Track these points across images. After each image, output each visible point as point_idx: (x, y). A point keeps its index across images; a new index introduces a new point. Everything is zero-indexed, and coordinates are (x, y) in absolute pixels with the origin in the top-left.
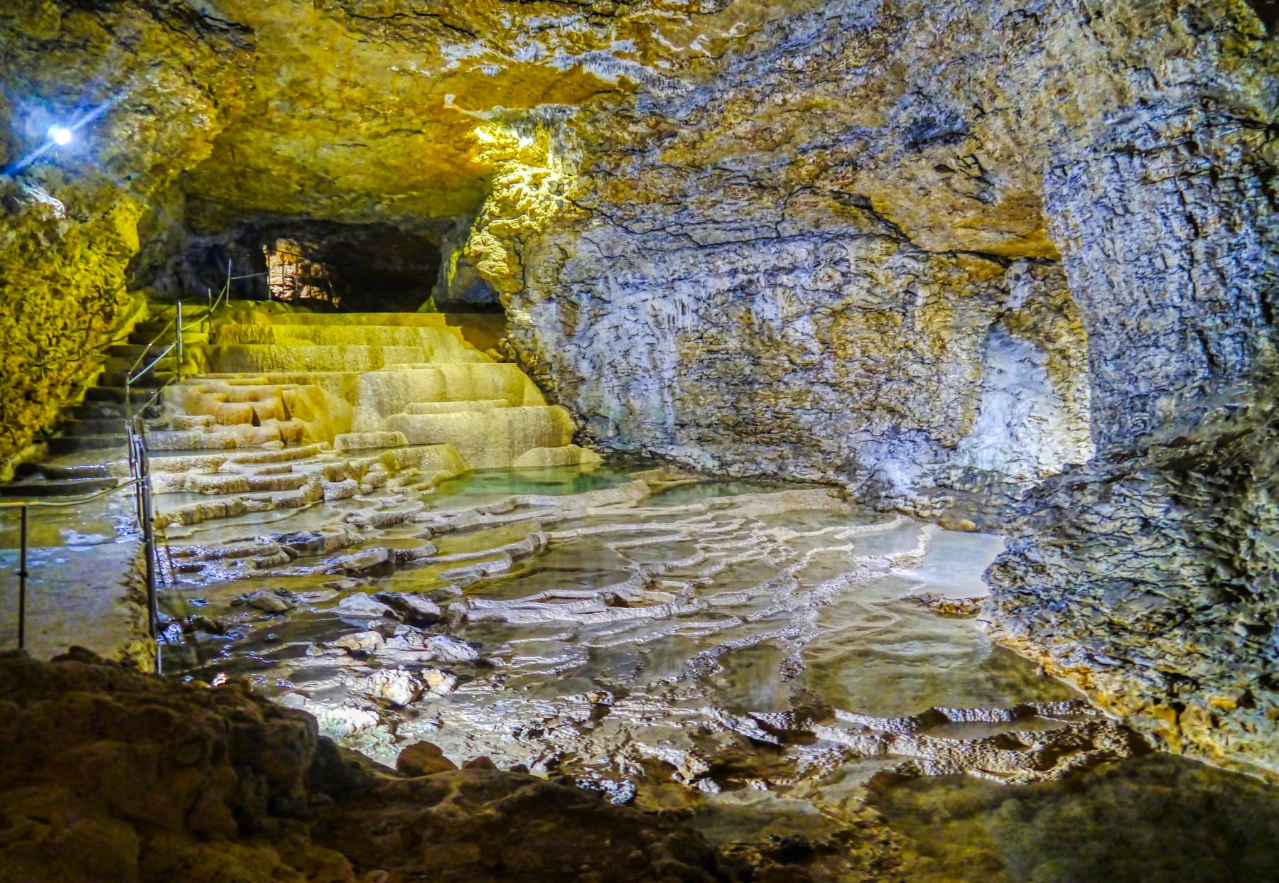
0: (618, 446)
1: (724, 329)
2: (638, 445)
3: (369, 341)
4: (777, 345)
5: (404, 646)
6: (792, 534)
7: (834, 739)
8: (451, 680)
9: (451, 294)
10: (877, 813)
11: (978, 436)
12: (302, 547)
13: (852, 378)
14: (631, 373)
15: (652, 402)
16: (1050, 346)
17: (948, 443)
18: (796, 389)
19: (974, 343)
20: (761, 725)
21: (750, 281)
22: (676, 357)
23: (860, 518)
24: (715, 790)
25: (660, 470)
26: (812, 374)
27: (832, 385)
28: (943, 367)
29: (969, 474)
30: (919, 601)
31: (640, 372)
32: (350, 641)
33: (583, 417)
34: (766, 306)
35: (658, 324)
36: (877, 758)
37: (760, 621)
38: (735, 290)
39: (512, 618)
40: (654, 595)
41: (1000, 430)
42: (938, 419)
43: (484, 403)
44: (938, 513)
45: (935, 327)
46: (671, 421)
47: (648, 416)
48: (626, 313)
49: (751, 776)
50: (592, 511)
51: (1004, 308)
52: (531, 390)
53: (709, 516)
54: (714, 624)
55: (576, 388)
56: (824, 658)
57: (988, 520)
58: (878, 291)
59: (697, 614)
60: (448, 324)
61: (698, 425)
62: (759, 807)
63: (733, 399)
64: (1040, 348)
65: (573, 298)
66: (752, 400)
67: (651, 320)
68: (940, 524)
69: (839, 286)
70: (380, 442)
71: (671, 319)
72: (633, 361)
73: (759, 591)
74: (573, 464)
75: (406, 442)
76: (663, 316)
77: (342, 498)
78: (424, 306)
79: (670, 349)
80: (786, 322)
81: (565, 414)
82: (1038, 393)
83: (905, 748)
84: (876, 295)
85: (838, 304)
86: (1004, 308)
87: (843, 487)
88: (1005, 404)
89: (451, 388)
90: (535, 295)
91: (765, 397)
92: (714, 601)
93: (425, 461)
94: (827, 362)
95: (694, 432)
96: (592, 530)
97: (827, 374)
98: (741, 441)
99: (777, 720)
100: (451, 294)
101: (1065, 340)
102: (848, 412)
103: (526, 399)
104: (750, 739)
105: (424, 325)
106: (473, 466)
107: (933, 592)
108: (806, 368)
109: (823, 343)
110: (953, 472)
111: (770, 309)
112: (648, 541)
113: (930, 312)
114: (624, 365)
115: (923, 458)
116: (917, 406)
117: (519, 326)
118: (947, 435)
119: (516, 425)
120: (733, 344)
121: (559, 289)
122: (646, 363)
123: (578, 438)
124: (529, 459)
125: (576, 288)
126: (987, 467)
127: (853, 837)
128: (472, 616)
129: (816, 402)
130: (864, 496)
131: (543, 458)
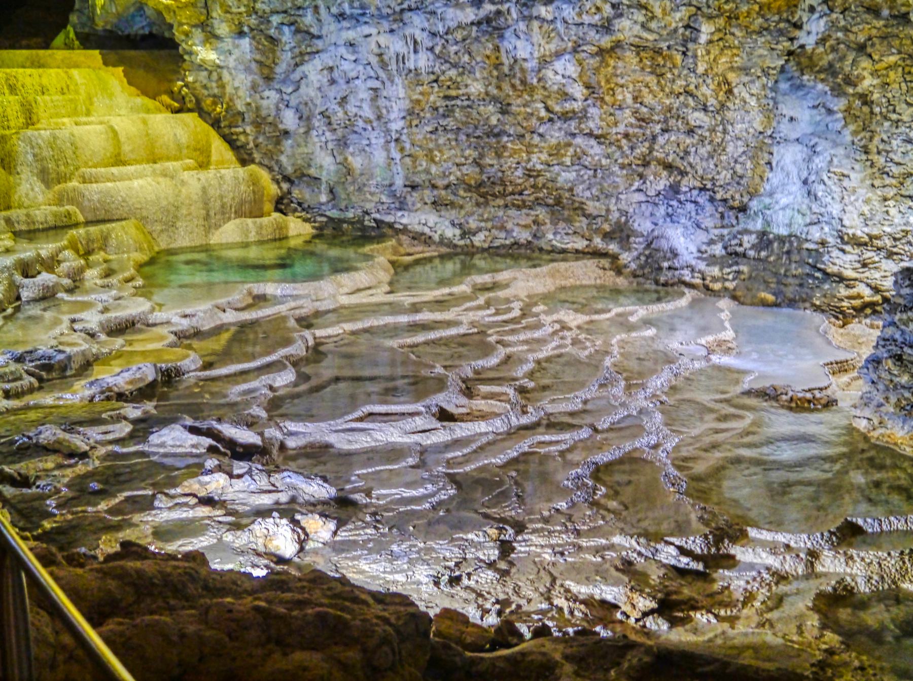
0: (334, 214)
1: (465, 70)
3: (13, 89)
4: (532, 90)
5: (253, 487)
6: (582, 319)
7: (757, 561)
8: (332, 525)
9: (100, 24)
10: (840, 639)
11: (771, 195)
12: (48, 368)
13: (621, 128)
14: (349, 124)
15: (375, 159)
16: (851, 90)
17: (736, 204)
18: (554, 141)
19: (764, 87)
20: (683, 551)
21: (499, 13)
22: (406, 104)
23: (640, 295)
24: (665, 627)
25: (393, 242)
26: (573, 124)
27: (597, 137)
28: (729, 115)
29: (764, 240)
30: (763, 394)
31: (361, 123)
32: (192, 485)
33: (287, 179)
34: (519, 44)
35: (384, 65)
36: (807, 577)
37: (610, 430)
38: (479, 23)
39: (341, 442)
40: (479, 404)
41: (796, 187)
42: (724, 176)
43: (170, 165)
44: (730, 285)
45: (720, 69)
46: (399, 182)
47: (372, 176)
48: (342, 50)
49: (695, 608)
50: (345, 300)
51: (796, 44)
52: (219, 148)
53: (481, 301)
54: (566, 436)
55: (278, 143)
56: (700, 468)
57: (790, 292)
58: (653, 25)
59: (537, 424)
60: (106, 63)
61: (434, 187)
62: (719, 641)
63: (475, 154)
64: (837, 91)
65: (272, 32)
66: (499, 156)
67: (374, 60)
68: (734, 298)
69: (609, 20)
70: (51, 221)
71: (401, 59)
72: (352, 109)
73: (591, 392)
74: (281, 238)
75: (81, 218)
76: (392, 53)
77: (43, 299)
78: (59, 39)
79: (398, 95)
80: (544, 62)
81: (264, 176)
82: (835, 144)
83: (832, 564)
84: (650, 30)
85: (606, 41)
86: (796, 44)
87: (615, 257)
88: (799, 157)
89: (126, 148)
90: (223, 29)
91: (515, 152)
92: (550, 408)
93: (113, 242)
94: (592, 111)
96: (359, 325)
97: (591, 124)
98: (487, 203)
99: (696, 544)
100: (100, 24)
101: (868, 82)
102: (616, 169)
103: (214, 157)
104: (674, 567)
105: (77, 66)
106: (163, 243)
107: (778, 383)
108: (566, 117)
109: (588, 87)
110: (746, 238)
111: (524, 47)
112: (432, 335)
113: (715, 51)
114: (341, 114)
115: (708, 223)
116: (699, 160)
117: (200, 67)
118: (737, 196)
119: (211, 192)
120: (476, 88)
121: (253, 21)
122: (368, 112)
123: (281, 205)
124: (230, 232)
125: (275, 20)
126: (784, 232)
127: (830, 665)
128: (291, 443)
129: (577, 158)
130: (642, 267)
131: (246, 232)
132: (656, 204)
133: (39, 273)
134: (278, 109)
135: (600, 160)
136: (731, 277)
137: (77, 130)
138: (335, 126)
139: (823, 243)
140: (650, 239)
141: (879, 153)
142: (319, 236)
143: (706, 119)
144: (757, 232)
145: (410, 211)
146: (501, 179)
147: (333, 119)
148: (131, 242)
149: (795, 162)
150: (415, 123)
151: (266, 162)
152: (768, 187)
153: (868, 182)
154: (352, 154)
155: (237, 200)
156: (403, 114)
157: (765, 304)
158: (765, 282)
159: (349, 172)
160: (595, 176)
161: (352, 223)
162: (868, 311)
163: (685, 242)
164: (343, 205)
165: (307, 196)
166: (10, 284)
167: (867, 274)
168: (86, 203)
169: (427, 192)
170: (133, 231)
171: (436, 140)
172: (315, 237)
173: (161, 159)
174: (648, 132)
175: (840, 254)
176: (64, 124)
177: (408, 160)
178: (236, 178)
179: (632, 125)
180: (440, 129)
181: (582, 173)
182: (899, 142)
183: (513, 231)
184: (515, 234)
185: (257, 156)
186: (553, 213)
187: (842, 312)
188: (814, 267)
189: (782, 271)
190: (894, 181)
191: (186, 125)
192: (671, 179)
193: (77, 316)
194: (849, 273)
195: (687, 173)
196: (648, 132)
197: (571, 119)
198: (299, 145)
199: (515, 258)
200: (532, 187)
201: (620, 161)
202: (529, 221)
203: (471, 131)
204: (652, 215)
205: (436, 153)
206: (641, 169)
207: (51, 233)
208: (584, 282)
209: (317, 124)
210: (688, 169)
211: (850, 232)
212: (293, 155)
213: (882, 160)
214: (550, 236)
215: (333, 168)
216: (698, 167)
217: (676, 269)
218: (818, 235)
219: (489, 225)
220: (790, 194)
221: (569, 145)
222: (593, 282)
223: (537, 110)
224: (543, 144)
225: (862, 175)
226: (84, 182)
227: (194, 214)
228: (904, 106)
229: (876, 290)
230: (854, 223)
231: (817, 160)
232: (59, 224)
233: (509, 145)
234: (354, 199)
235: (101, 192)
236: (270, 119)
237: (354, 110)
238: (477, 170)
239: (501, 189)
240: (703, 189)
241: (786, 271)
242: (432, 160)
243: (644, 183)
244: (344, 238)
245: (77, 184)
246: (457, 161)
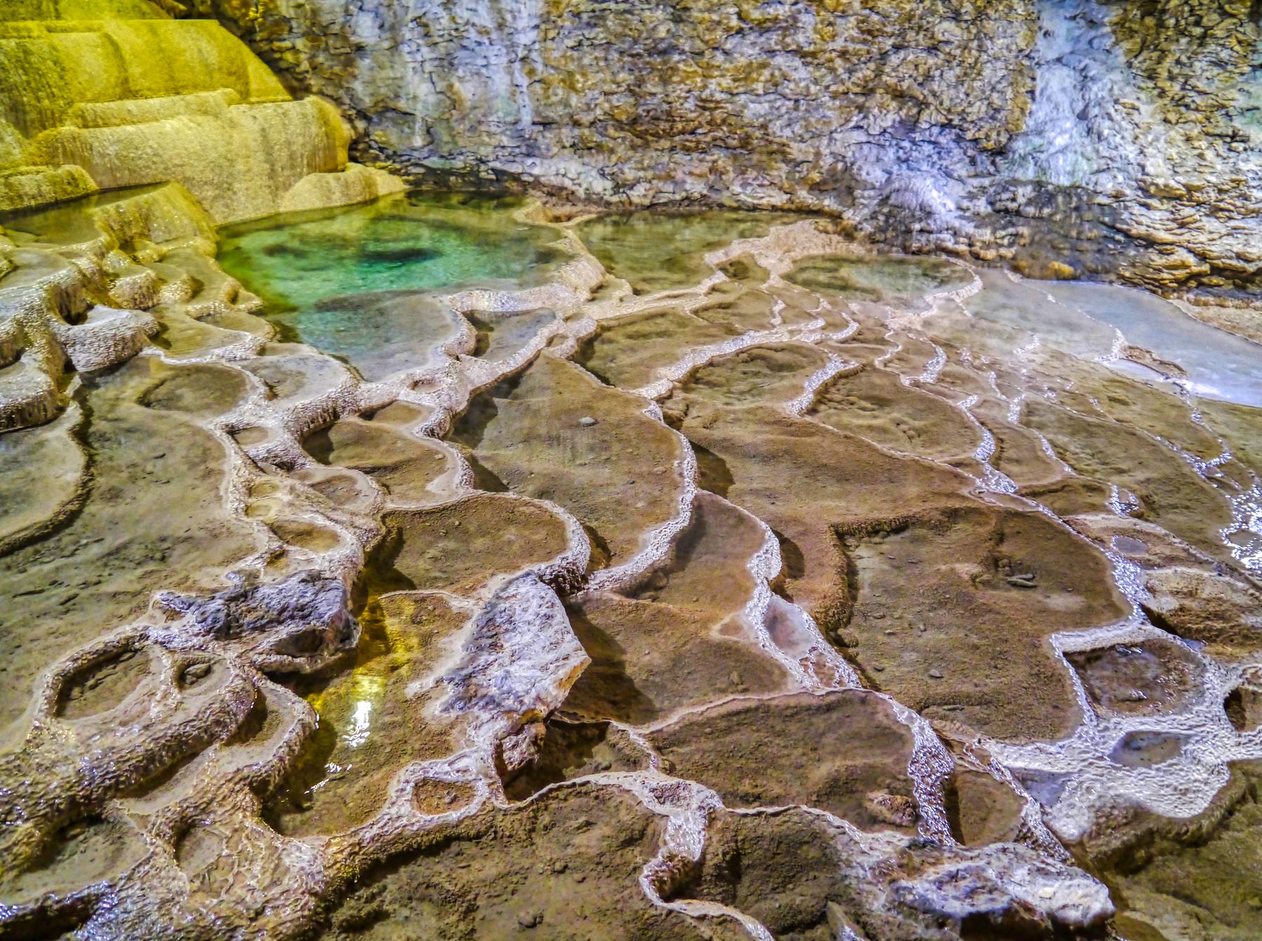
0: (434, 162)
2: (471, 160)
13: (839, 44)
14: (456, 36)
15: (497, 88)
17: (991, 145)
18: (743, 61)
26: (775, 37)
27: (803, 55)
28: (989, 26)
29: (1044, 194)
31: (473, 34)
33: (362, 115)
42: (978, 109)
44: (1009, 253)
46: (527, 118)
52: (257, 70)
55: (349, 63)
57: (1089, 259)
61: (577, 124)
66: (665, 81)
68: (1016, 269)
70: (49, 194)
75: (93, 185)
82: (1111, 69)
87: (836, 217)
88: (1068, 83)
89: (135, 70)
91: (689, 75)
94: (805, 19)
95: (567, 135)
97: (801, 38)
98: (647, 145)
106: (220, 220)
108: (763, 27)
110: (1020, 191)
114: (445, 21)
116: (945, 87)
119: (274, 136)
123: (358, 150)
124: (306, 193)
126: (1065, 181)
130: (883, 230)
132: (883, 146)
133: (90, 307)
134: (347, 13)
135: (807, 87)
136: (1006, 241)
137: (57, 39)
138: (438, 40)
139: (1118, 196)
140: (887, 191)
141: (1172, 78)
142: (413, 195)
143: (958, 31)
144: (1031, 182)
145: (543, 157)
146: (669, 113)
147: (434, 28)
148: (186, 221)
149: (1064, 90)
150: (552, 34)
151: (330, 90)
152: (1031, 123)
153: (1161, 116)
154: (460, 79)
155: (309, 147)
156: (536, 22)
157: (1060, 277)
158: (1054, 247)
159: (455, 104)
160: (796, 109)
161: (463, 176)
162: (1193, 284)
163: (941, 196)
164: (445, 150)
165: (394, 139)
166: (49, 343)
167: (1187, 237)
168: (97, 160)
169: (565, 131)
170: (182, 203)
171: (580, 59)
172: (409, 195)
173: (184, 87)
174: (874, 49)
175: (1144, 210)
176: (29, 30)
177: (538, 87)
178: (305, 116)
179: (853, 40)
180: (586, 43)
181: (778, 103)
182: (1204, 64)
183: (684, 182)
184: (688, 187)
185: (314, 82)
186: (735, 158)
187: (1162, 286)
188: (1113, 227)
189: (1074, 233)
190: (1200, 116)
191: (212, 36)
192: (903, 113)
193: (231, 418)
195: (928, 105)
196: (874, 49)
197: (768, 30)
198: (381, 67)
199: (687, 217)
200: (709, 123)
201: (833, 88)
202: (704, 168)
203: (626, 46)
204: (878, 160)
205: (578, 77)
206: (861, 99)
207: (52, 214)
208: (814, 252)
209: (408, 36)
210: (931, 99)
211: (1161, 181)
212: (373, 82)
213: (1177, 87)
214: (737, 189)
215: (432, 99)
216: (944, 97)
217: (930, 232)
218: (1110, 185)
219: (650, 174)
220: (1062, 132)
221: (764, 66)
222: (822, 252)
223: (728, 16)
224: (727, 65)
225: (1152, 107)
226: (86, 126)
227: (255, 169)
228: (1215, 17)
229: (1203, 257)
230: (1159, 171)
231: (1095, 88)
232: (61, 197)
233: (681, 66)
234: (461, 142)
235: (119, 141)
236: (336, 28)
237: (467, 15)
238: (632, 100)
239: (667, 125)
240: (947, 125)
241: (1079, 233)
242: (572, 87)
243: (865, 117)
244: (455, 199)
245: (73, 128)
246: (606, 88)
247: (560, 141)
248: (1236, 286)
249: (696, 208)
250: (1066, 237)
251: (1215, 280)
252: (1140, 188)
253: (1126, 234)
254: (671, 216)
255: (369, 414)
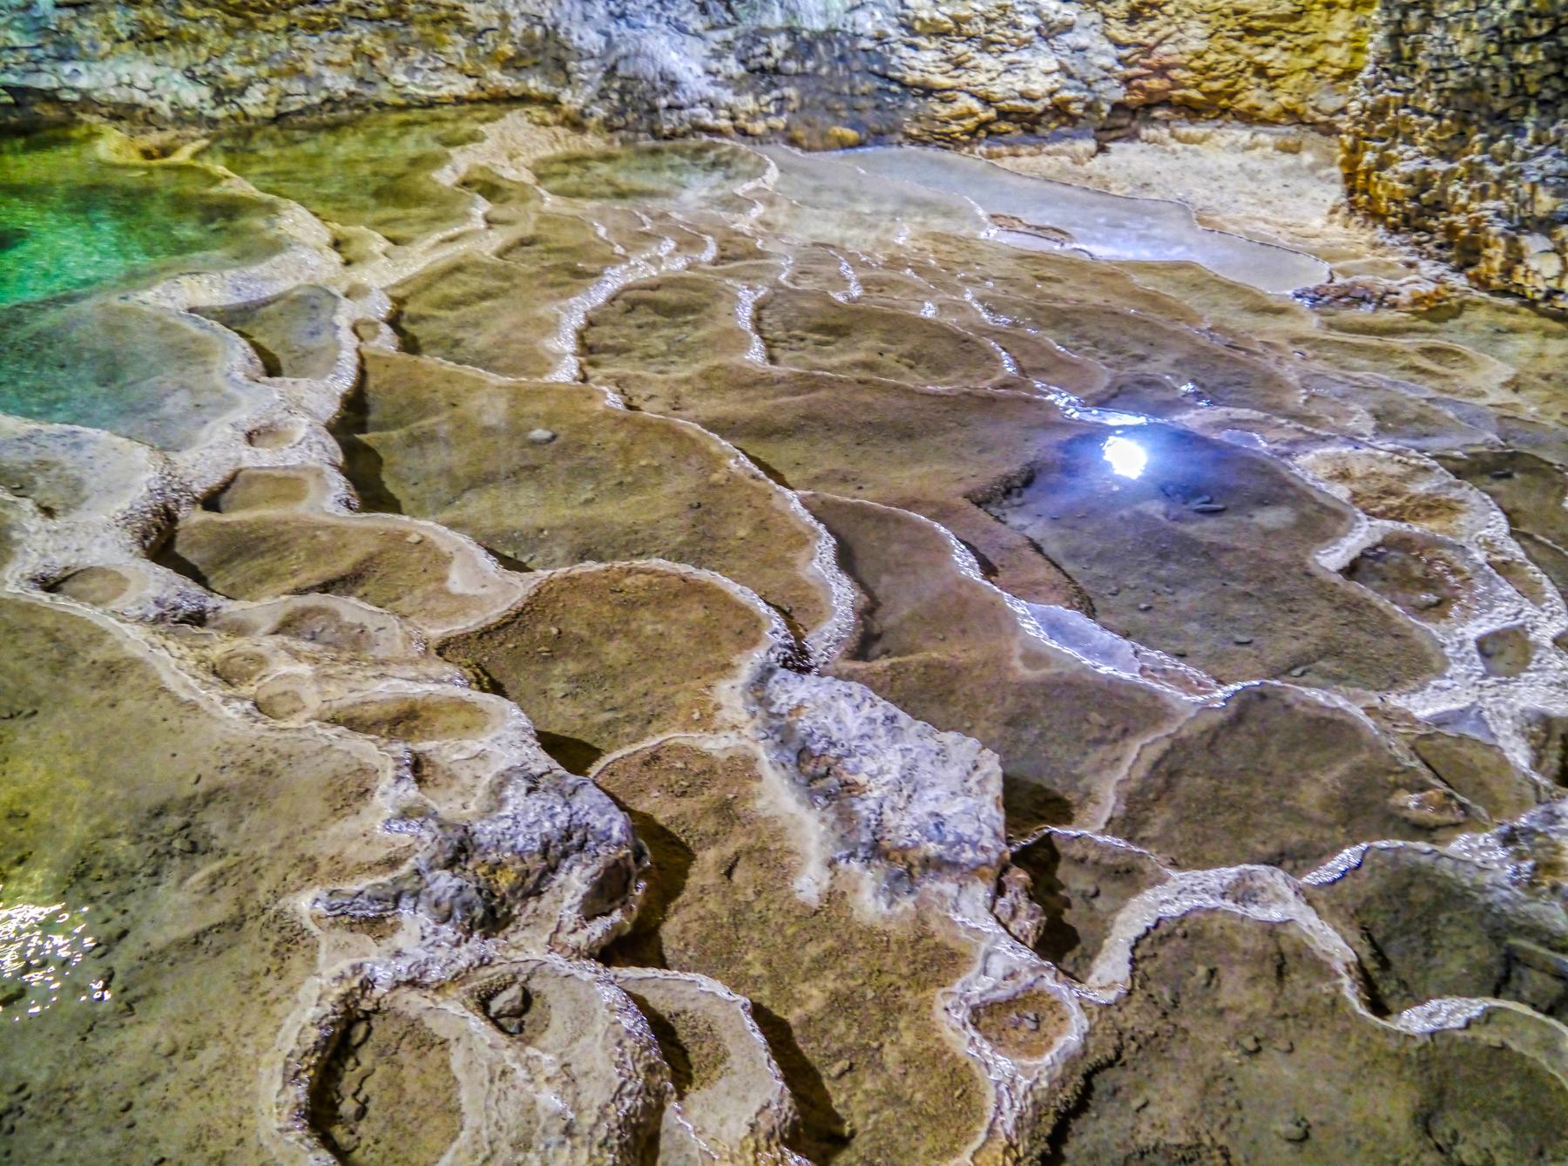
44: (779, 122)
68: (793, 142)
98: (250, 25)
126: (819, 25)
136: (772, 109)
139: (880, 38)
140: (610, 61)
145: (87, 58)
157: (844, 145)
158: (829, 109)
167: (965, 79)
175: (912, 53)
184: (328, 82)
186: (386, 34)
188: (884, 77)
189: (846, 89)
194: (940, 80)
199: (334, 127)
202: (343, 53)
204: (586, 18)
211: (924, 15)
214: (400, 77)
217: (680, 108)
218: (869, 25)
219: (264, 70)
229: (987, 101)
241: (852, 88)
247: (110, 31)
248: (1025, 130)
249: (345, 113)
250: (838, 94)
251: (1004, 126)
252: (902, 25)
253: (900, 83)
254: (314, 129)
255: (211, 502)
